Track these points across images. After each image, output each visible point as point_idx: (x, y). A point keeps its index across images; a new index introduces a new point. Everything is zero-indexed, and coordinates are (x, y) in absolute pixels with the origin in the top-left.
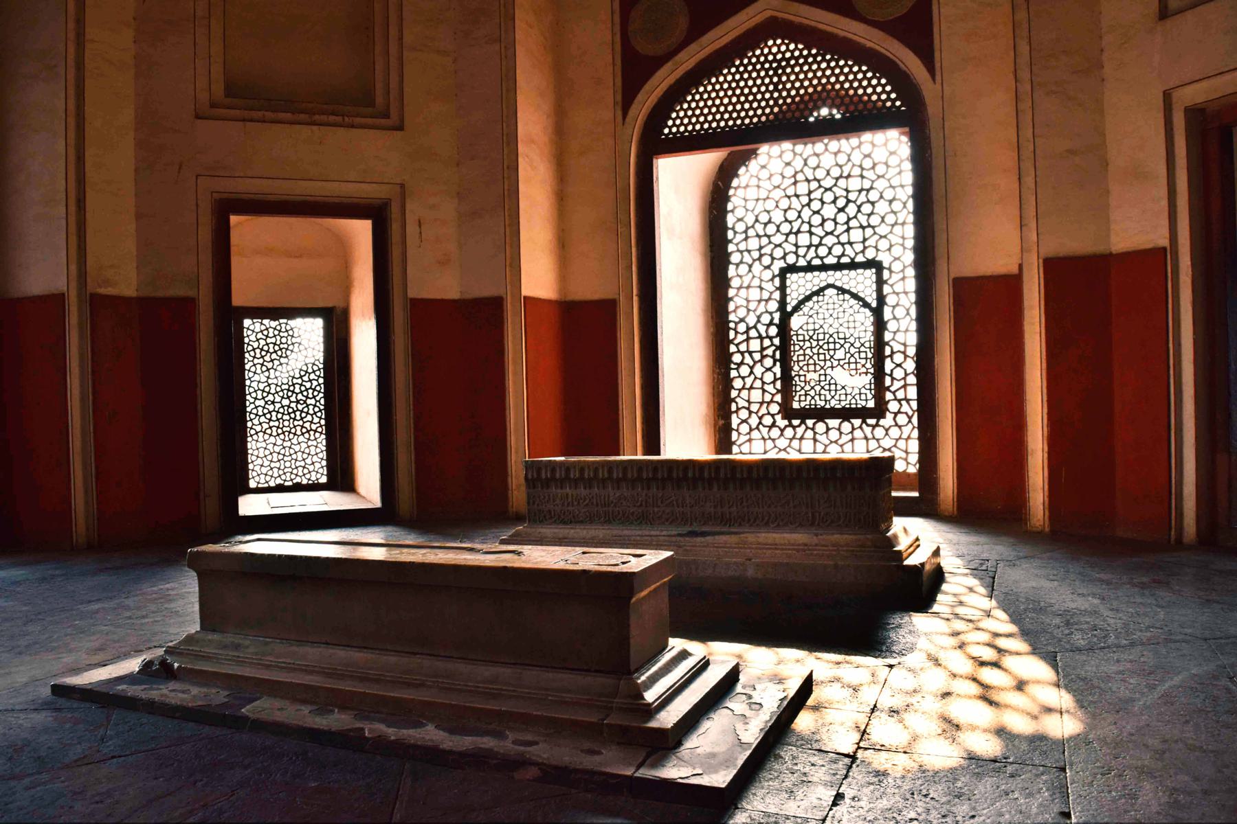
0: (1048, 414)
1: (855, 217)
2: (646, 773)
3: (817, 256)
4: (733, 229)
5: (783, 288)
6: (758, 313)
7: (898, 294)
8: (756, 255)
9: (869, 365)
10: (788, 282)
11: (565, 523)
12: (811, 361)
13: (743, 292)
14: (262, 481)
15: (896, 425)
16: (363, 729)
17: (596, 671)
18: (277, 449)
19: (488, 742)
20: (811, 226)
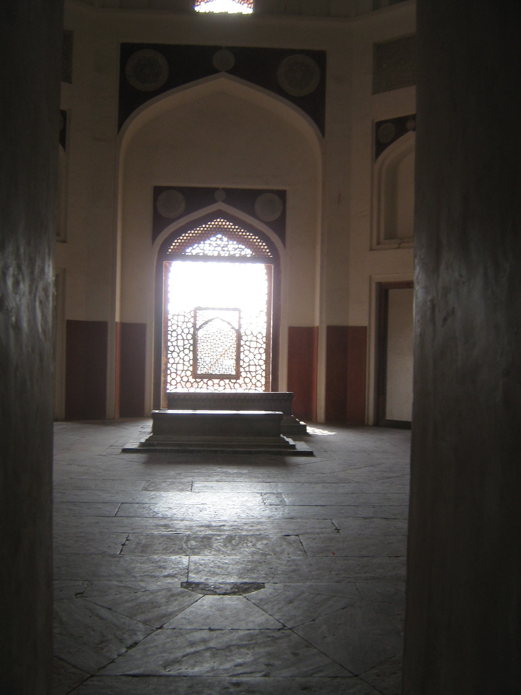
10: (198, 314)
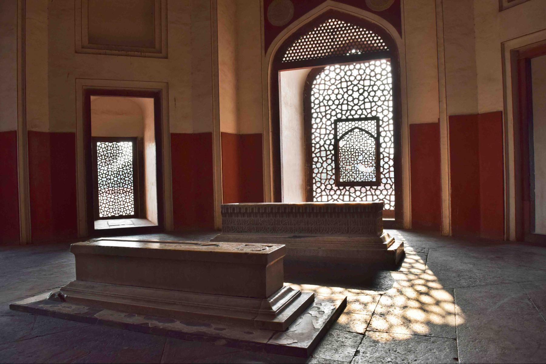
0: (451, 184)
1: (367, 97)
2: (272, 342)
3: (351, 115)
4: (314, 102)
5: (335, 129)
6: (325, 139)
7: (386, 131)
8: (324, 114)
9: (373, 163)
10: (338, 126)
11: (239, 232)
12: (348, 161)
13: (318, 131)
14: (105, 214)
15: (385, 189)
16: (148, 323)
17: (251, 297)
18: (112, 200)
19: (203, 329)
20: (348, 101)
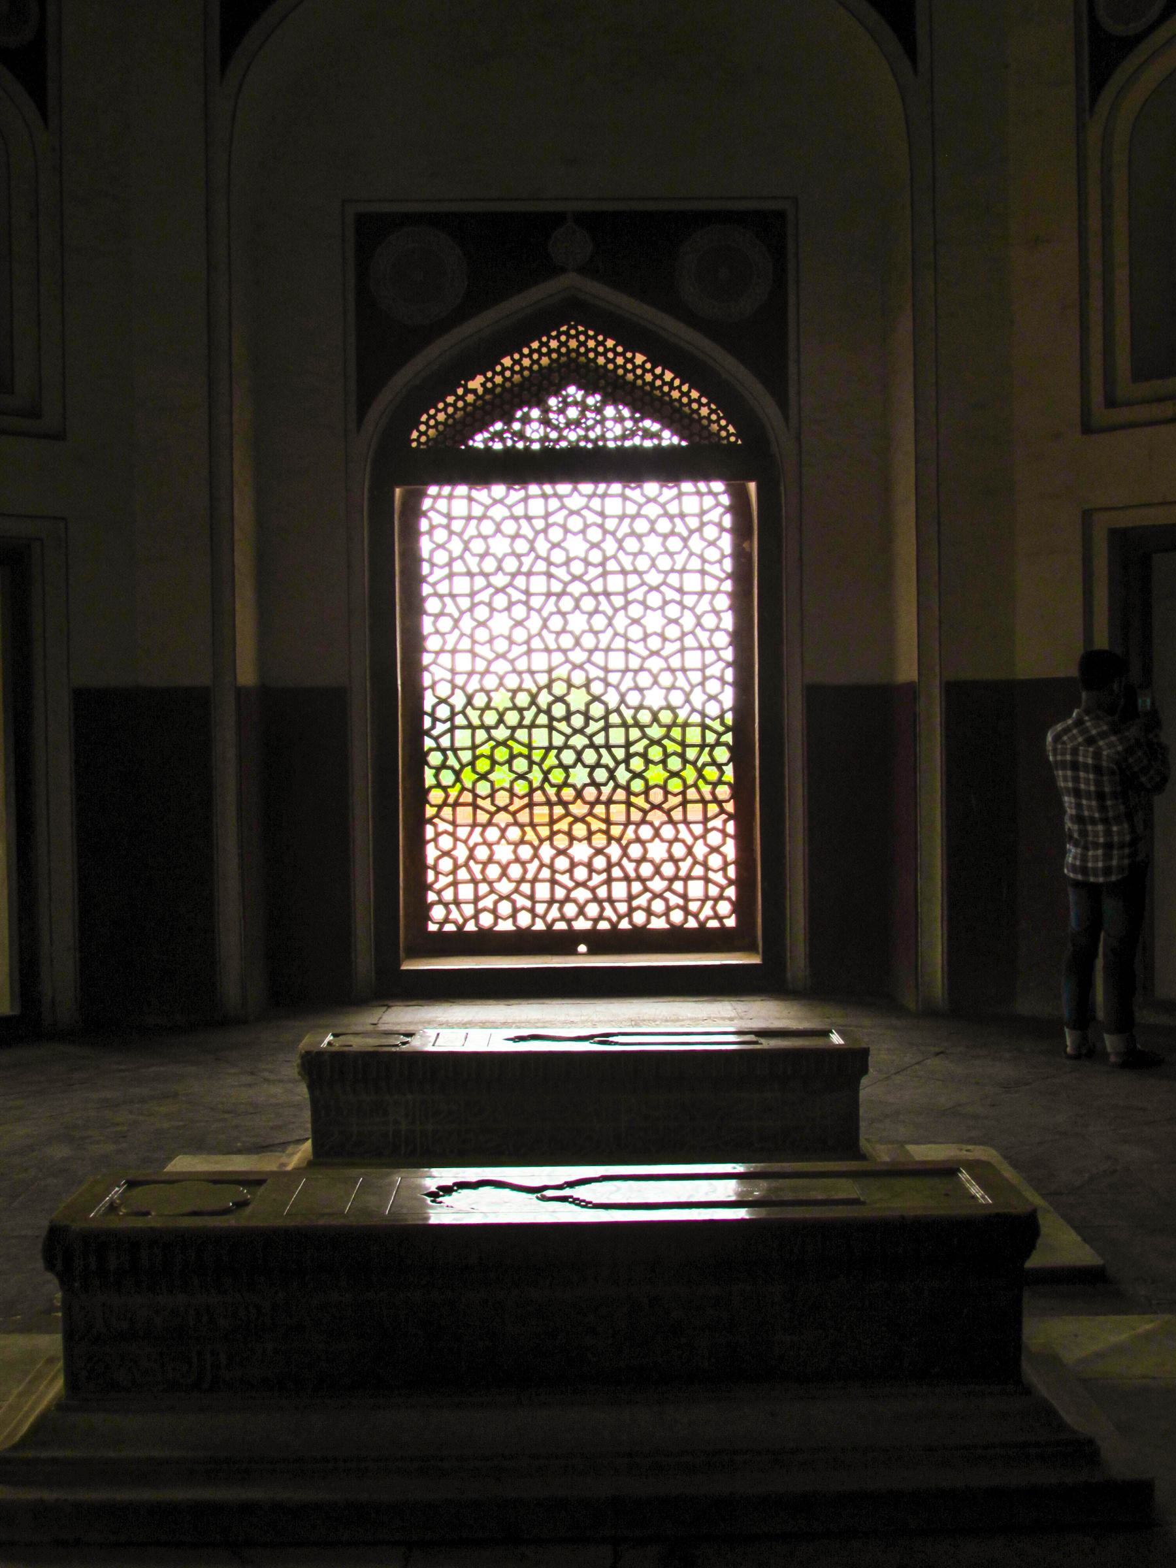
13: (445, 659)
